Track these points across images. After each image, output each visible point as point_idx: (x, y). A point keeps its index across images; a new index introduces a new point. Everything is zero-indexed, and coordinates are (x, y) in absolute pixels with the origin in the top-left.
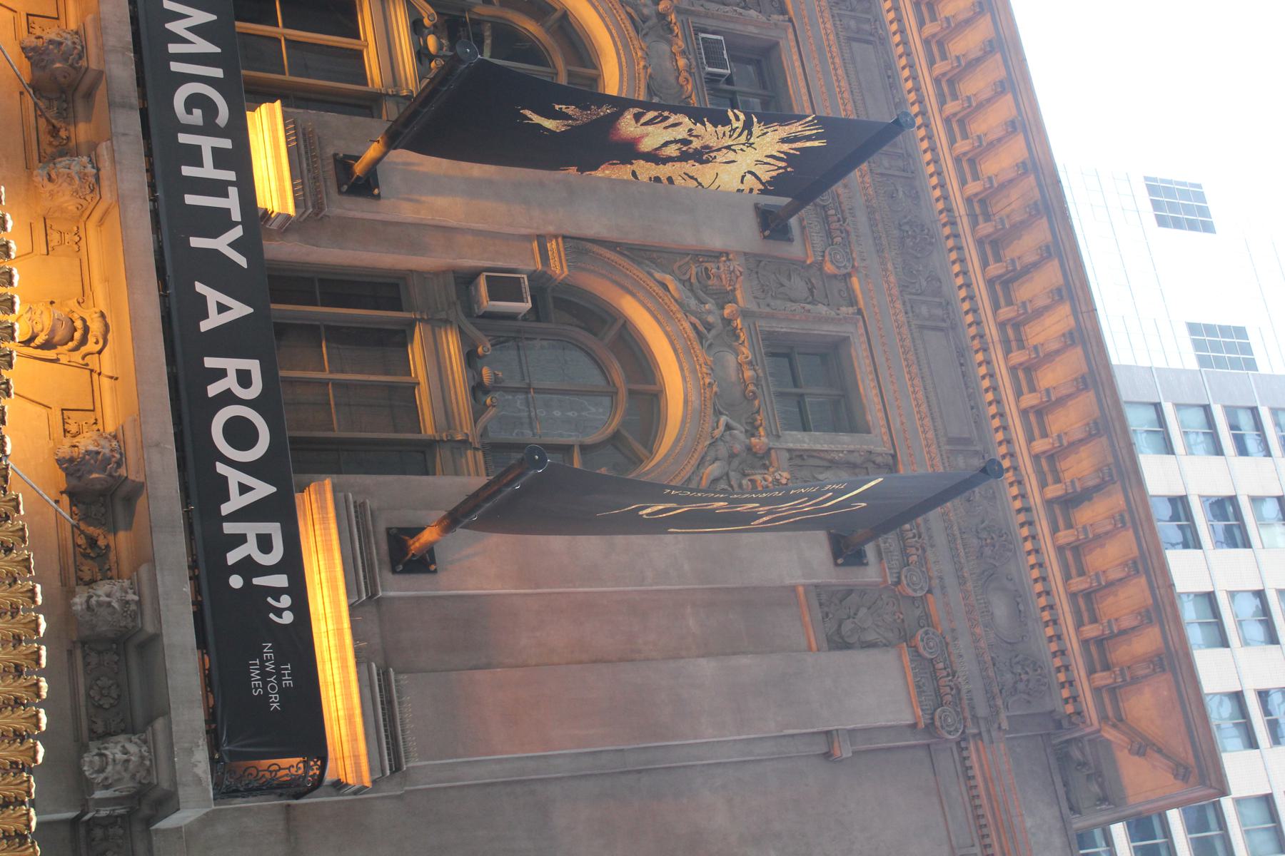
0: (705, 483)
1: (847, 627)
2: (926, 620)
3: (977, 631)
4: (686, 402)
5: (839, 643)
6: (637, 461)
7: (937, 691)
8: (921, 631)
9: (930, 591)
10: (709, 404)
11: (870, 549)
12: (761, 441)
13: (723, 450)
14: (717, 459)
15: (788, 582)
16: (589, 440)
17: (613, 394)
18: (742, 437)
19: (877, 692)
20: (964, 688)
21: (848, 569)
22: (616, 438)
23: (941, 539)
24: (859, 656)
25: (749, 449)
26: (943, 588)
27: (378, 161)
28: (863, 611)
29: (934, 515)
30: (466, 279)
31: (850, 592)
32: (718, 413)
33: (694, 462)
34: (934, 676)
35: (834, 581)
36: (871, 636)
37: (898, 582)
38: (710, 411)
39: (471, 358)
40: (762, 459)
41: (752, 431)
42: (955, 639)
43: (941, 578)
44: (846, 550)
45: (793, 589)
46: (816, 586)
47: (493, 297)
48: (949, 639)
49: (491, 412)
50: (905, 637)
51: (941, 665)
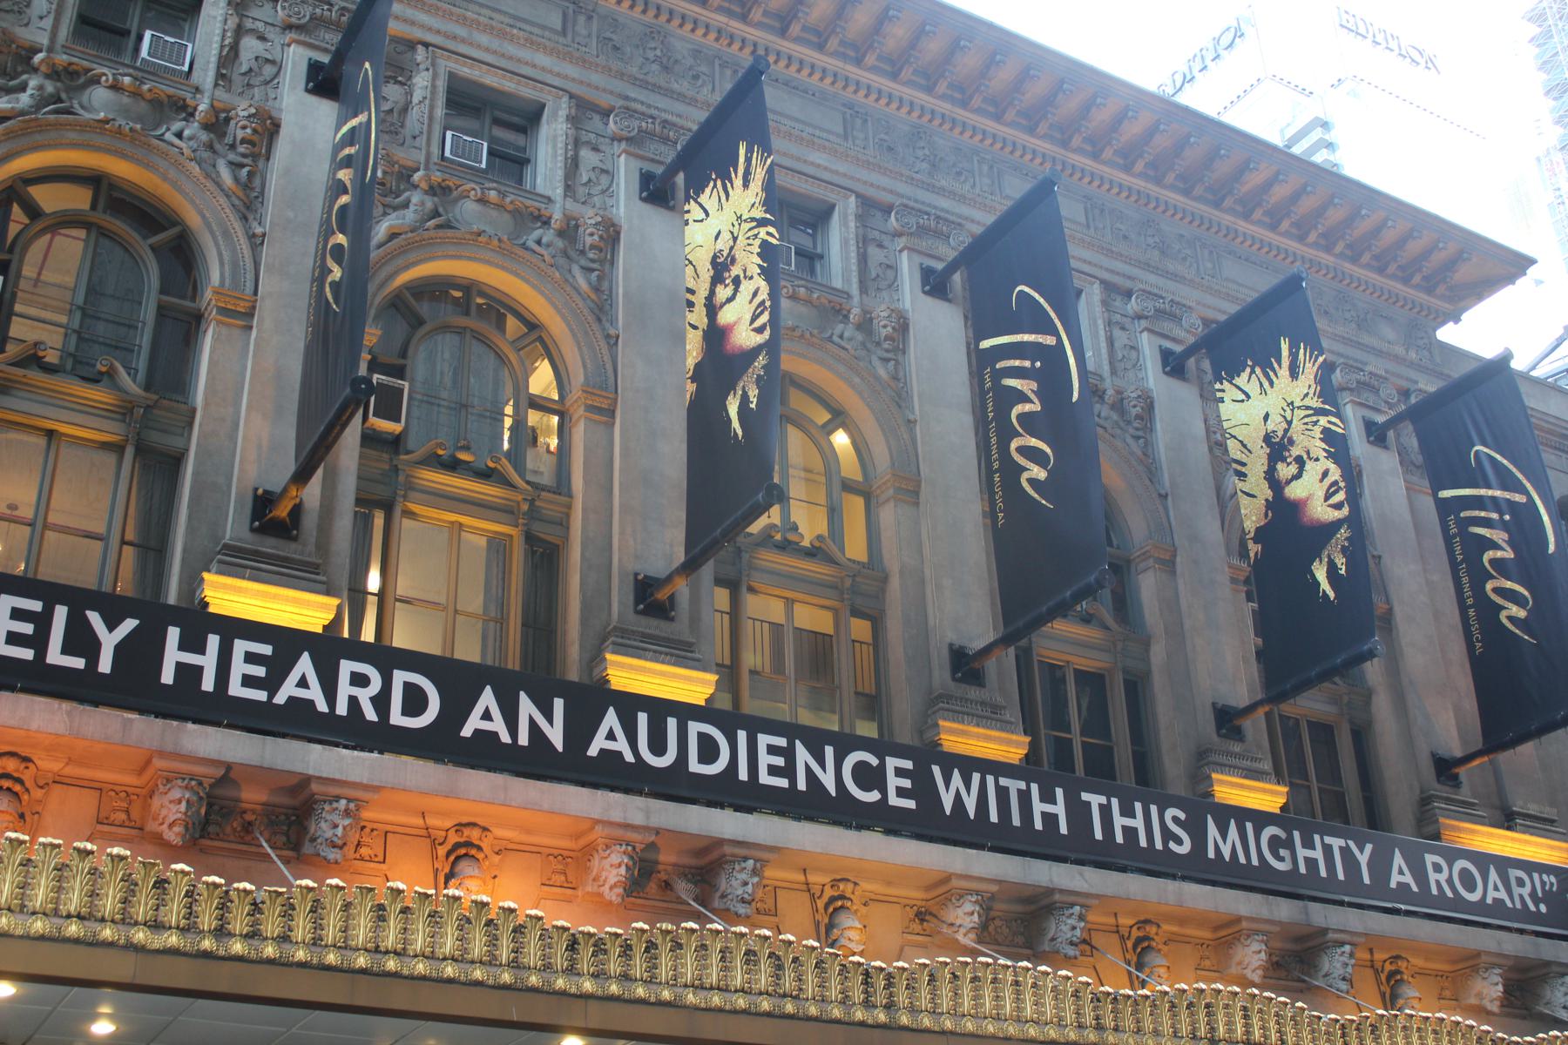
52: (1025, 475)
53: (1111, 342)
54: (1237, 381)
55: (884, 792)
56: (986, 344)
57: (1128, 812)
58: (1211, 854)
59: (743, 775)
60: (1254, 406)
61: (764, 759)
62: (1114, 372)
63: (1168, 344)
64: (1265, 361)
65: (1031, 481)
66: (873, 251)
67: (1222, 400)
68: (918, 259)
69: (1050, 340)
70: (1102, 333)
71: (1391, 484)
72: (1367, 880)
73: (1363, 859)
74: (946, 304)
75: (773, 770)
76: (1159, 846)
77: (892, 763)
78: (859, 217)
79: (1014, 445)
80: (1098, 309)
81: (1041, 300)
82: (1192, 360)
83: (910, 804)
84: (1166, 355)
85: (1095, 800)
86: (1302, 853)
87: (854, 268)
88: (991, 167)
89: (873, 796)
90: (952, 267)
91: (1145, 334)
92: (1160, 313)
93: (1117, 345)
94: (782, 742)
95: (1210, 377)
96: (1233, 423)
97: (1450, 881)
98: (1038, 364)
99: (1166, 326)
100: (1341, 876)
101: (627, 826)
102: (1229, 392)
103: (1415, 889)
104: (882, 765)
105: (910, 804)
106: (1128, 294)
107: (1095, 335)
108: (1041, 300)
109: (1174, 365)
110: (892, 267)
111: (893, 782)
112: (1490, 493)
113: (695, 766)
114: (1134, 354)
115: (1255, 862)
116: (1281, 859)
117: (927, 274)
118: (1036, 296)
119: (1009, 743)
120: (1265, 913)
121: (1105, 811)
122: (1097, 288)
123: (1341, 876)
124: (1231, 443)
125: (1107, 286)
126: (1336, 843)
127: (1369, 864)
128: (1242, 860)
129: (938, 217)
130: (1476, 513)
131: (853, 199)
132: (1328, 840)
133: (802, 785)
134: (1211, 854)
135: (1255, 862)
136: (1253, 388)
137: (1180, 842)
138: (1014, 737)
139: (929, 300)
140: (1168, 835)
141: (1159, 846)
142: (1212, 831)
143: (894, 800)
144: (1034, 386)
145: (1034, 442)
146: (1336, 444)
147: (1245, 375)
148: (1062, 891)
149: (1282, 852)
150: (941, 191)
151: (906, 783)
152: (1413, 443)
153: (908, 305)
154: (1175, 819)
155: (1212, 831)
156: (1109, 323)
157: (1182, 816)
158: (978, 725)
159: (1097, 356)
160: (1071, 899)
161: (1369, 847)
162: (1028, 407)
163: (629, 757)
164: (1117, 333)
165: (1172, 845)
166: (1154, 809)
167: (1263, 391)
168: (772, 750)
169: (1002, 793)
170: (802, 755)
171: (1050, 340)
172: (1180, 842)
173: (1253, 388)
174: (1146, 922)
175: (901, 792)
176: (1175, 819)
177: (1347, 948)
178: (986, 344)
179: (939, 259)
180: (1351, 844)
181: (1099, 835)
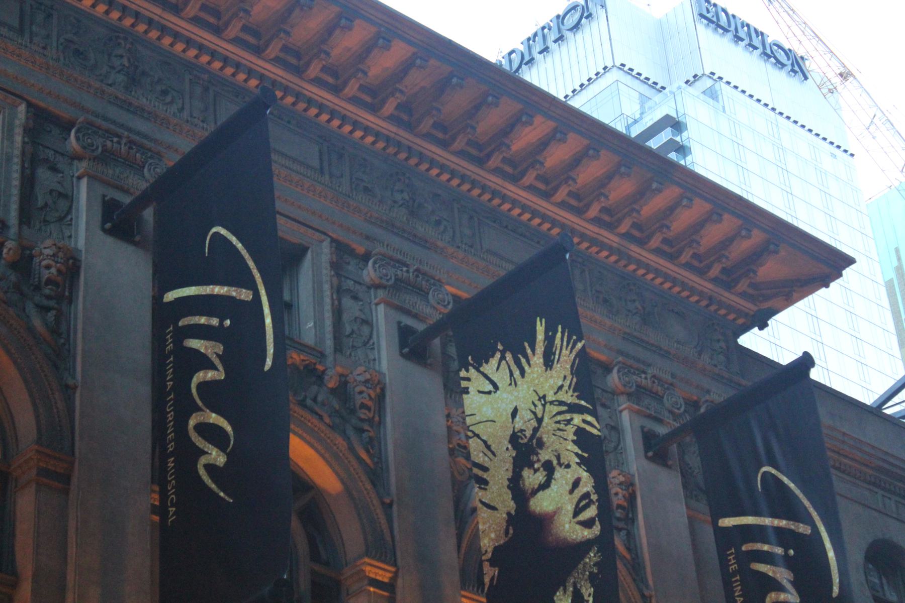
52: (203, 460)
53: (338, 313)
54: (486, 368)
56: (171, 296)
60: (504, 397)
62: (338, 348)
63: (408, 321)
64: (517, 346)
65: (211, 468)
66: (43, 174)
67: (466, 391)
68: (100, 190)
69: (245, 295)
70: (328, 300)
71: (665, 508)
74: (131, 248)
78: (27, 131)
79: (192, 423)
80: (326, 272)
81: (239, 246)
82: (437, 342)
84: (405, 333)
87: (15, 192)
88: (206, 89)
90: (143, 200)
91: (381, 308)
92: (400, 285)
93: (345, 317)
95: (455, 365)
96: (478, 418)
98: (228, 322)
99: (409, 300)
102: (475, 382)
106: (366, 258)
107: (318, 302)
108: (239, 246)
109: (413, 347)
110: (69, 198)
112: (776, 522)
114: (366, 330)
117: (109, 209)
118: (234, 240)
122: (326, 248)
124: (474, 445)
125: (340, 247)
129: (131, 142)
130: (759, 546)
131: (22, 108)
136: (501, 377)
139: (110, 240)
144: (220, 348)
145: (214, 418)
146: (595, 453)
147: (494, 362)
150: (139, 111)
152: (694, 461)
153: (81, 244)
156: (339, 291)
159: (311, 325)
162: (210, 375)
164: (347, 302)
167: (513, 382)
171: (245, 295)
173: (501, 377)
178: (171, 296)
179: (126, 192)
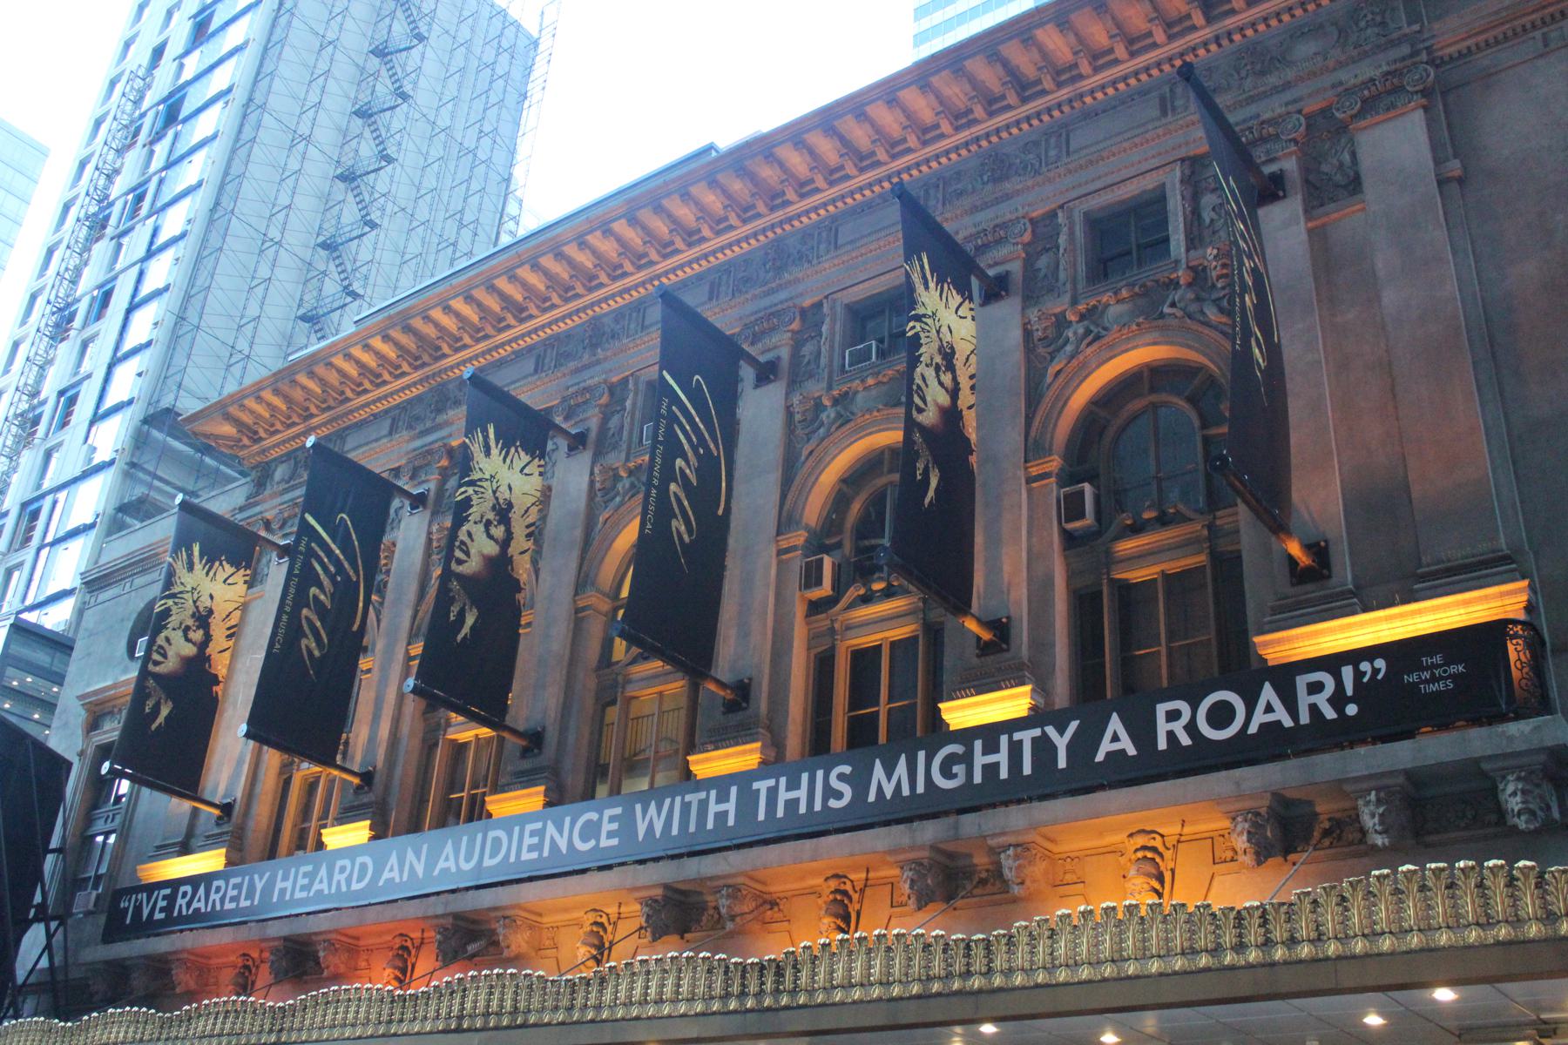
0: (1224, 319)
1: (1339, 178)
2: (1325, 112)
3: (1331, 63)
4: (1155, 343)
5: (1355, 185)
6: (1212, 380)
7: (1389, 93)
8: (1337, 115)
9: (1300, 112)
10: (1155, 323)
11: (1268, 170)
12: (1182, 275)
13: (1193, 308)
14: (1202, 312)
15: (1304, 237)
16: (1197, 423)
17: (1155, 407)
18: (1180, 292)
19: (1398, 145)
20: (1385, 68)
21: (1288, 187)
22: (1191, 400)
23: (1252, 110)
24: (1366, 162)
25: (1189, 285)
26: (1295, 101)
27: (979, 621)
28: (1325, 168)
29: (1232, 118)
30: (1070, 540)
31: (1307, 181)
32: (1162, 316)
33: (1207, 331)
34: (1376, 98)
35: (1299, 197)
36: (1347, 157)
37: (1295, 141)
38: (1160, 322)
39: (1137, 529)
40: (1199, 275)
41: (1174, 284)
42: (1341, 83)
43: (1287, 104)
44: (1271, 190)
45: (1310, 231)
46: (1306, 211)
47: (1082, 515)
48: (1340, 89)
49: (1181, 507)
50: (1342, 128)
51: (1366, 92)
55: (598, 841)
57: (793, 785)
58: (872, 798)
59: (512, 859)
61: (528, 841)
72: (1062, 763)
73: (1061, 742)
75: (531, 848)
76: (818, 807)
77: (608, 813)
83: (615, 842)
85: (762, 786)
86: (980, 760)
89: (593, 843)
94: (539, 825)
97: (1191, 728)
100: (1027, 770)
101: (437, 917)
103: (1132, 751)
104: (601, 819)
105: (615, 842)
111: (607, 827)
113: (488, 862)
115: (920, 789)
116: (955, 776)
119: (744, 753)
120: (906, 841)
121: (773, 793)
123: (1027, 770)
126: (1026, 736)
127: (1069, 747)
128: (906, 792)
132: (1017, 736)
133: (546, 854)
134: (872, 798)
135: (920, 789)
137: (839, 795)
138: (748, 747)
140: (830, 793)
141: (818, 807)
142: (878, 771)
143: (605, 842)
148: (711, 879)
149: (955, 769)
151: (615, 826)
154: (841, 777)
155: (878, 771)
157: (847, 769)
158: (717, 748)
160: (721, 882)
161: (1074, 725)
163: (453, 869)
165: (833, 803)
166: (820, 774)
168: (532, 834)
169: (686, 807)
170: (551, 829)
172: (839, 795)
174: (836, 876)
175: (610, 835)
176: (841, 777)
177: (1011, 852)
180: (1051, 731)
181: (761, 817)
